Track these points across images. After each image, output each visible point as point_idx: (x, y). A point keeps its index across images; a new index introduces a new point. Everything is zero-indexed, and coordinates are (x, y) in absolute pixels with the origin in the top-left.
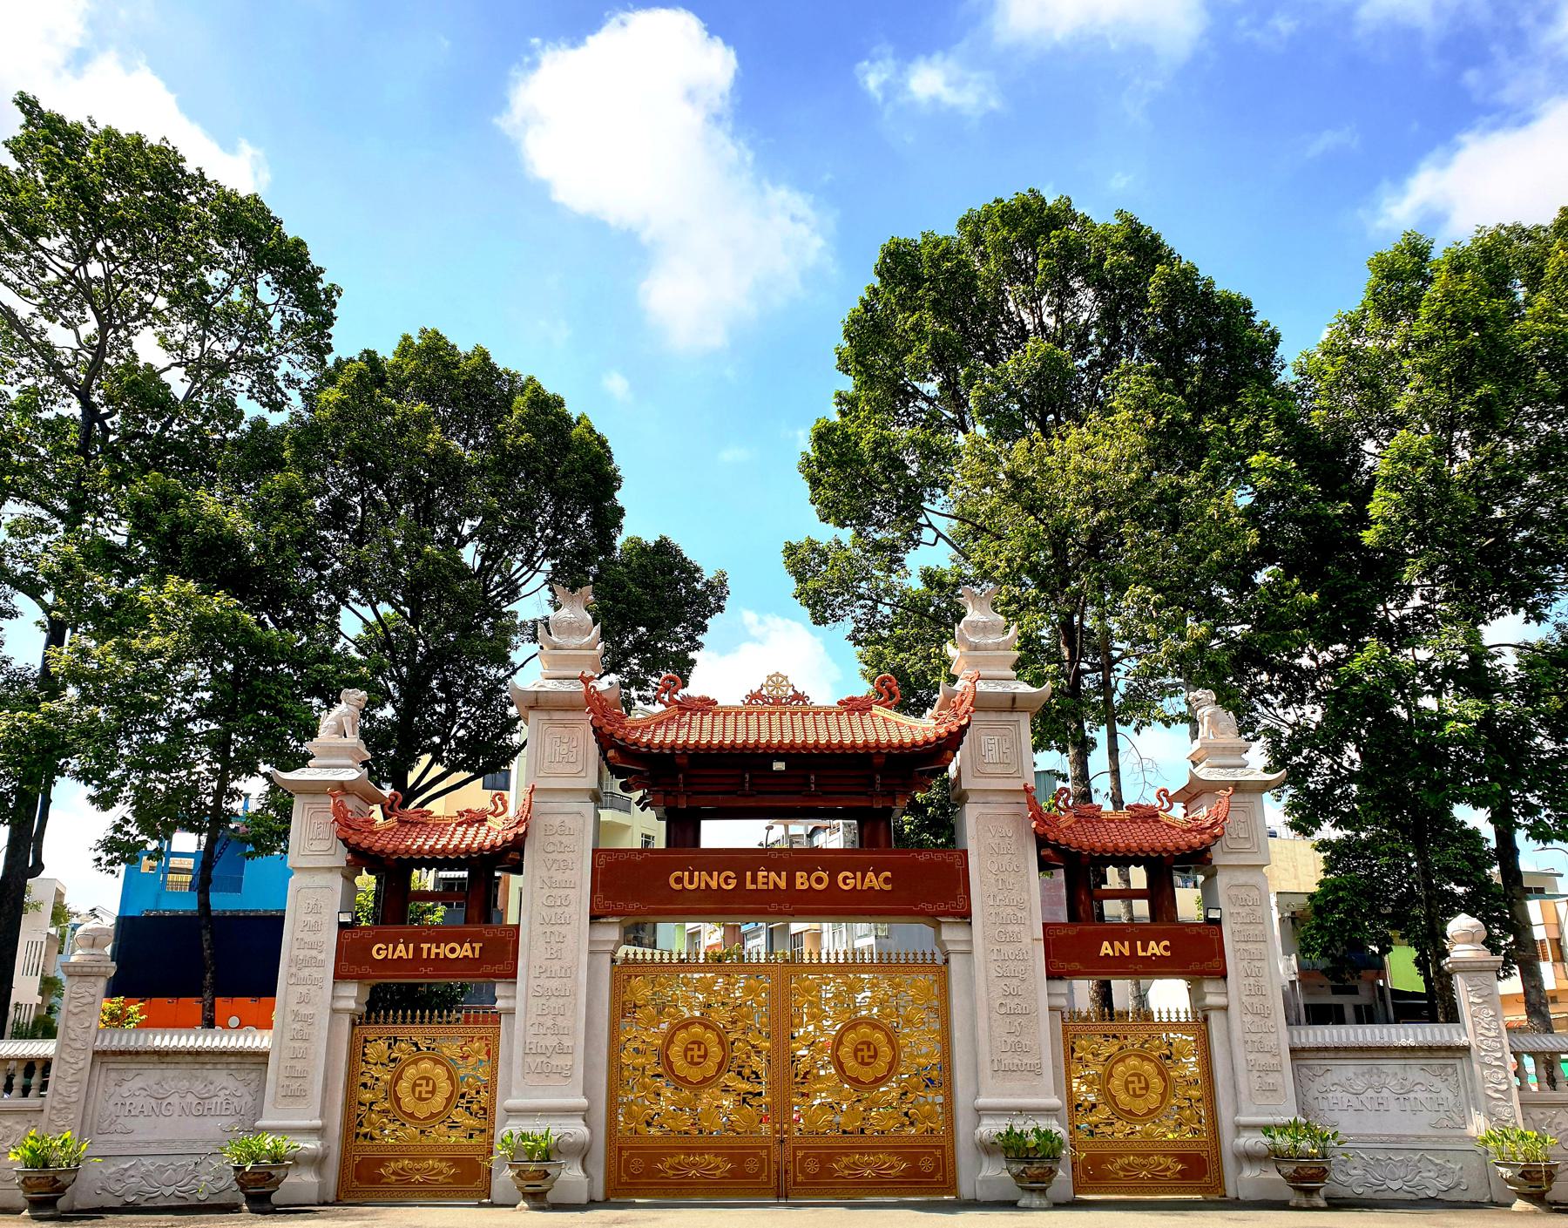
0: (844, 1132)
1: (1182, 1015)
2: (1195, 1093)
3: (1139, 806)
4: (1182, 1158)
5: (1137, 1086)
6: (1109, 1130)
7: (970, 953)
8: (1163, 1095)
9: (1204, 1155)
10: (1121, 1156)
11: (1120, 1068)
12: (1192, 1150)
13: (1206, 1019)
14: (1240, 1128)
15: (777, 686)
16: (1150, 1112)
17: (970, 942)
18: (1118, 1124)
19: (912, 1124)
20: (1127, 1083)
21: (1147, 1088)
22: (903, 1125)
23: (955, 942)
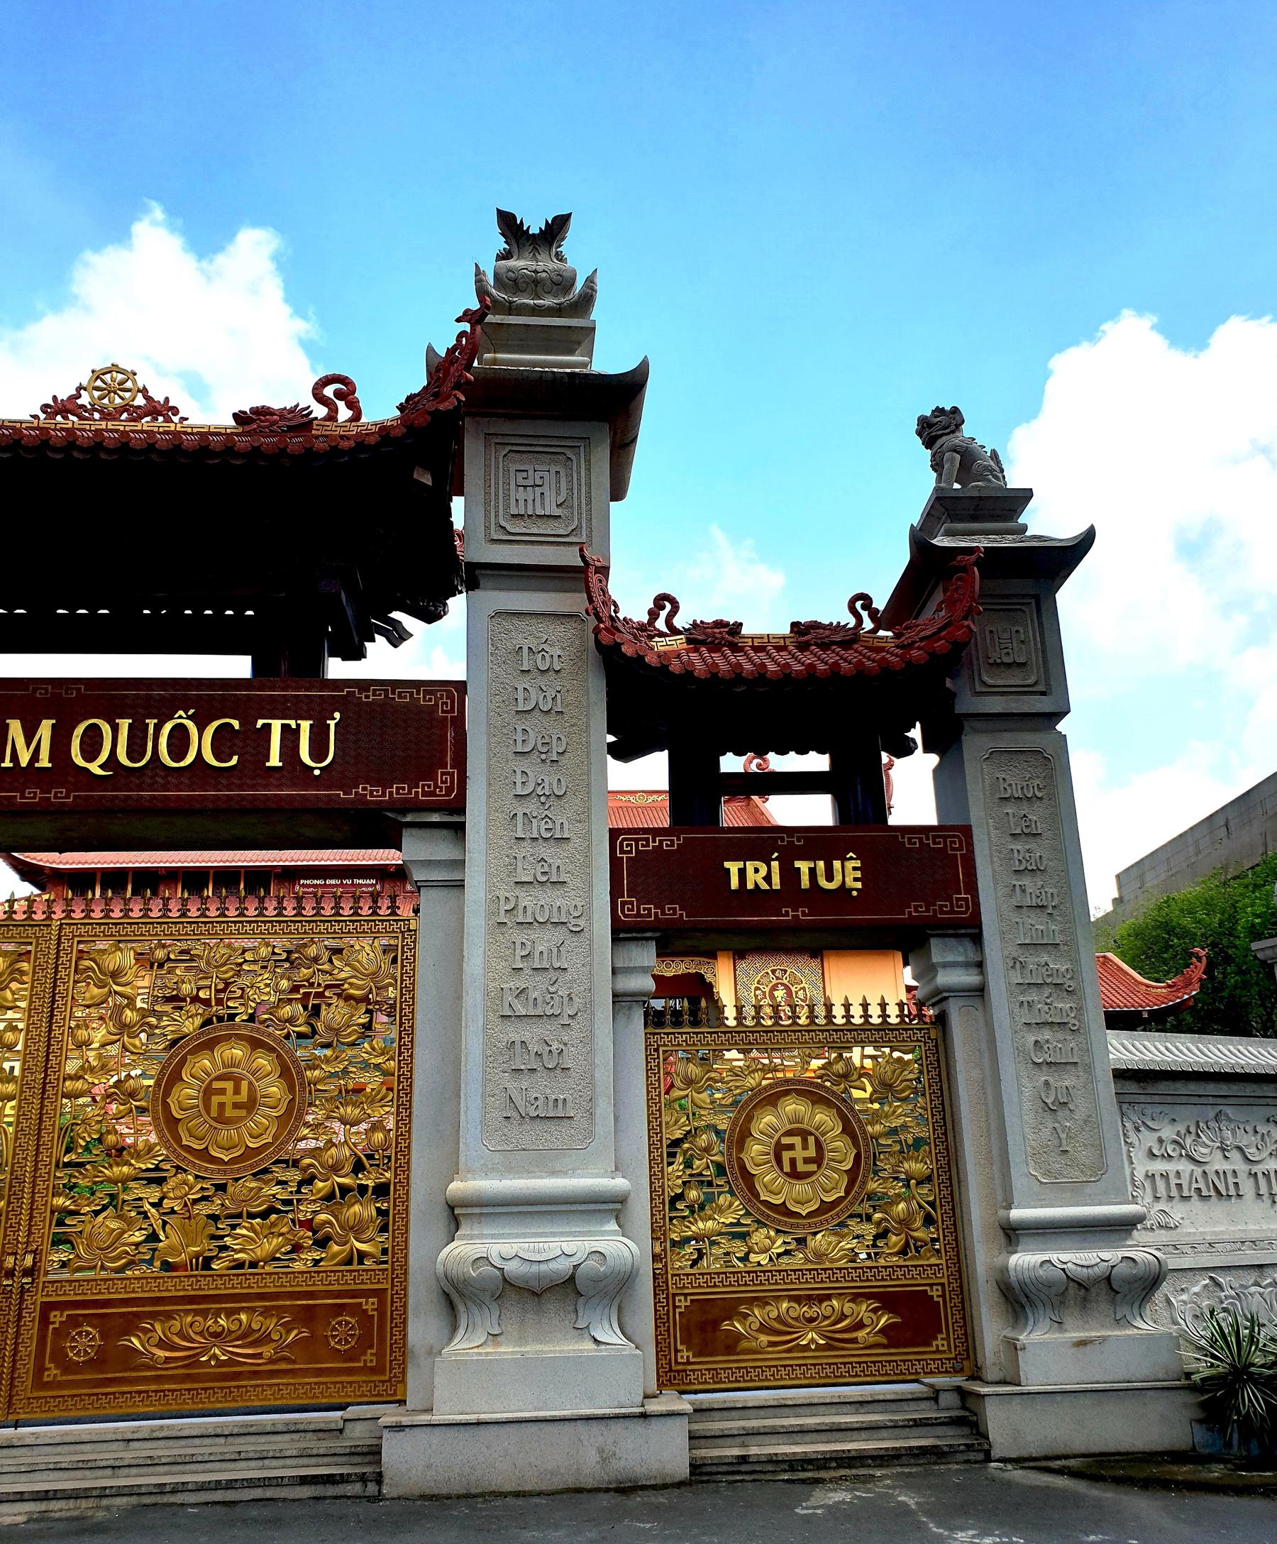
0: (167, 1266)
1: (893, 1011)
2: (915, 1167)
3: (815, 625)
4: (887, 1301)
5: (799, 1154)
6: (739, 1248)
7: (460, 885)
8: (853, 1174)
9: (935, 1293)
10: (763, 1302)
11: (767, 1119)
12: (914, 1282)
13: (942, 1020)
14: (1012, 1234)
15: (109, 391)
16: (825, 1208)
17: (461, 864)
18: (759, 1237)
19: (322, 1243)
20: (779, 1149)
21: (818, 1160)
22: (297, 1248)
23: (429, 864)
